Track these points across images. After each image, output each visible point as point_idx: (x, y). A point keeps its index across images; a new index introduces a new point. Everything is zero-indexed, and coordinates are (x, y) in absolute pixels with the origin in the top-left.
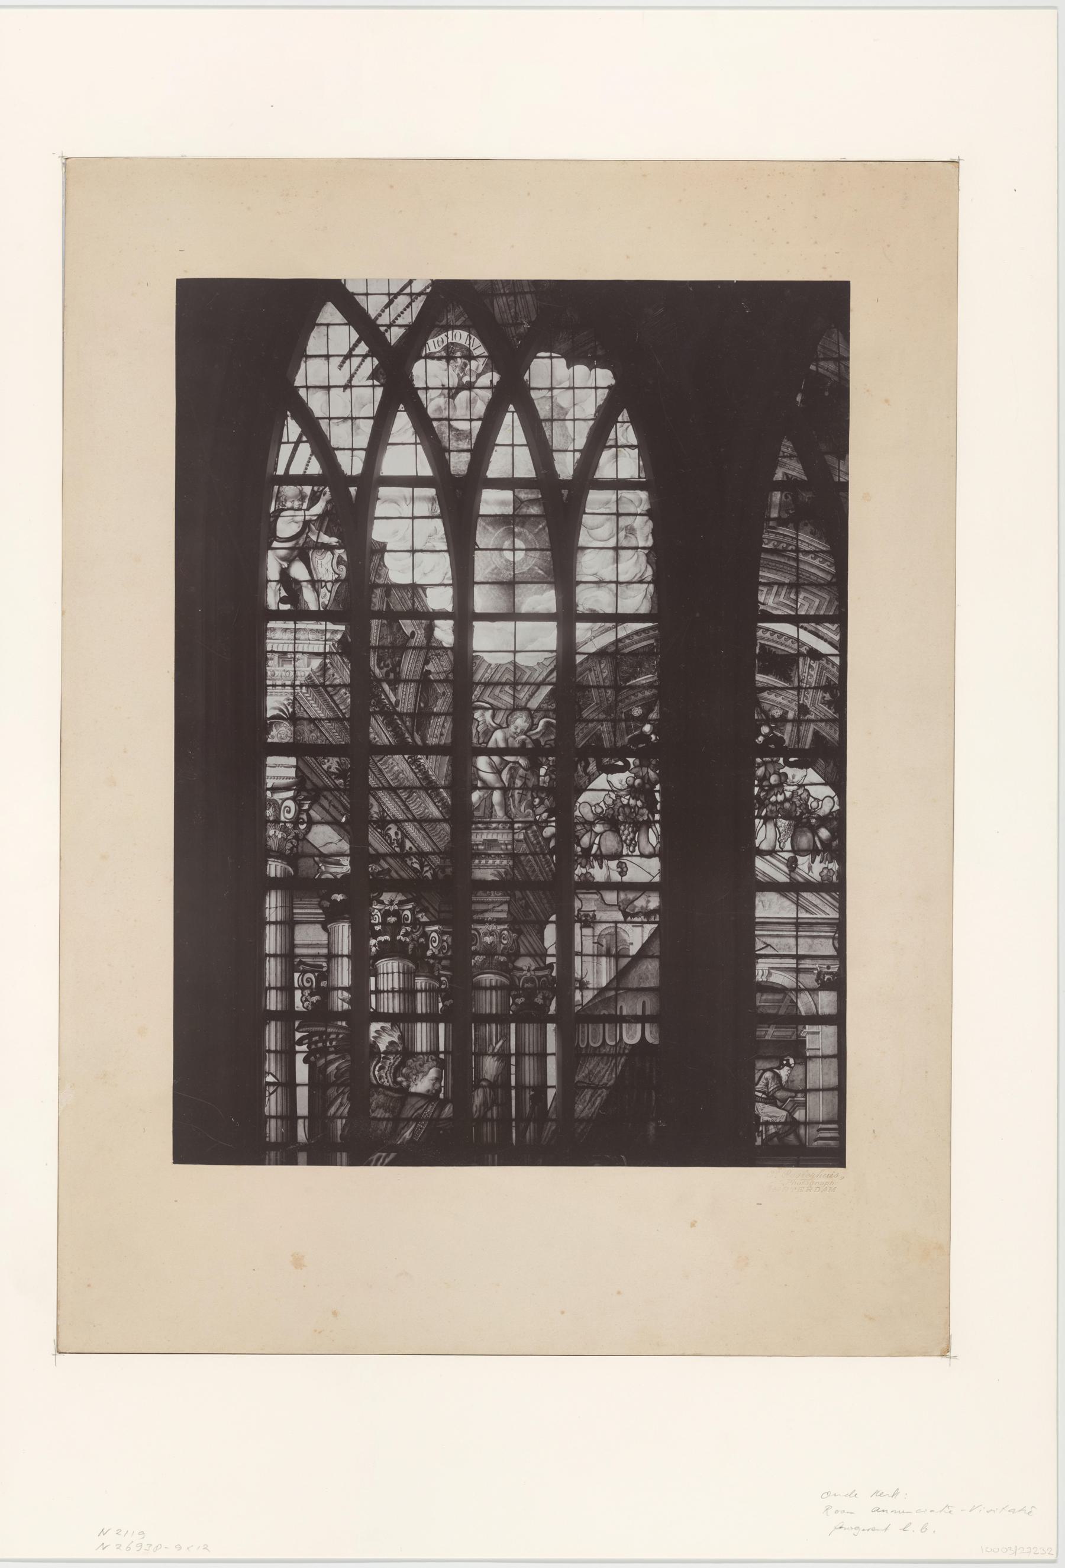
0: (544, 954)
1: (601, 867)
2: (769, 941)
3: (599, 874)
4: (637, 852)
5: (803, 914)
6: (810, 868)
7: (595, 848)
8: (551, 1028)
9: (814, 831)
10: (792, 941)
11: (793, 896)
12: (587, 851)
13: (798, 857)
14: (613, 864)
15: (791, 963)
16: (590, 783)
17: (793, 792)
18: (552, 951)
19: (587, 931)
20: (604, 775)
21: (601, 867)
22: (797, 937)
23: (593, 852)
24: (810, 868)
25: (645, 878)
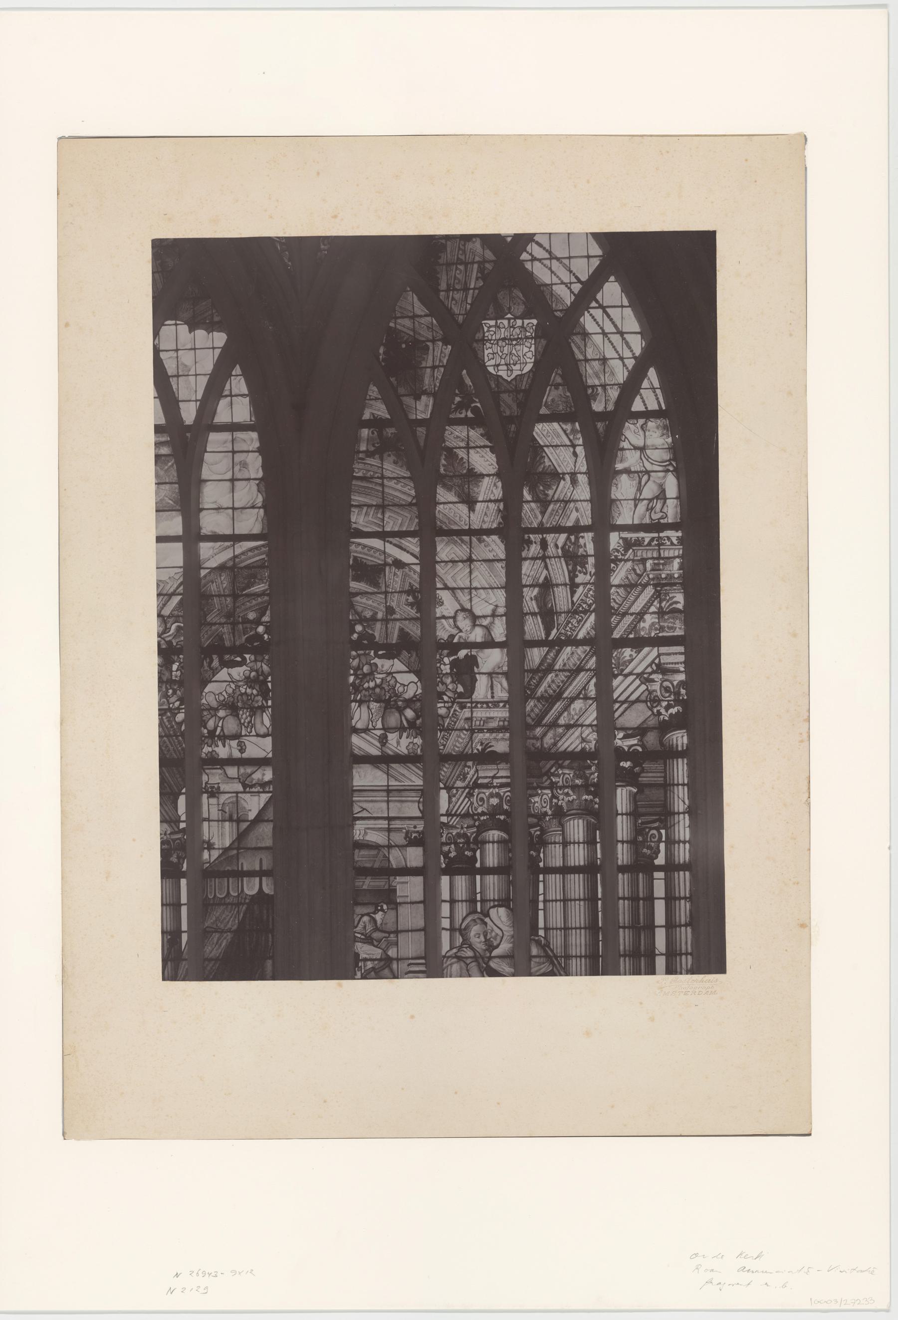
0: (179, 821)
1: (224, 746)
2: (365, 805)
3: (222, 752)
4: (253, 733)
5: (393, 782)
6: (398, 743)
7: (219, 730)
8: (183, 882)
9: (401, 711)
10: (384, 805)
11: (384, 766)
12: (212, 733)
13: (387, 733)
14: (234, 743)
15: (384, 824)
16: (214, 676)
17: (382, 679)
18: (183, 818)
19: (213, 801)
20: (225, 669)
21: (224, 746)
22: (388, 802)
23: (217, 733)
24: (398, 743)
25: (262, 754)
